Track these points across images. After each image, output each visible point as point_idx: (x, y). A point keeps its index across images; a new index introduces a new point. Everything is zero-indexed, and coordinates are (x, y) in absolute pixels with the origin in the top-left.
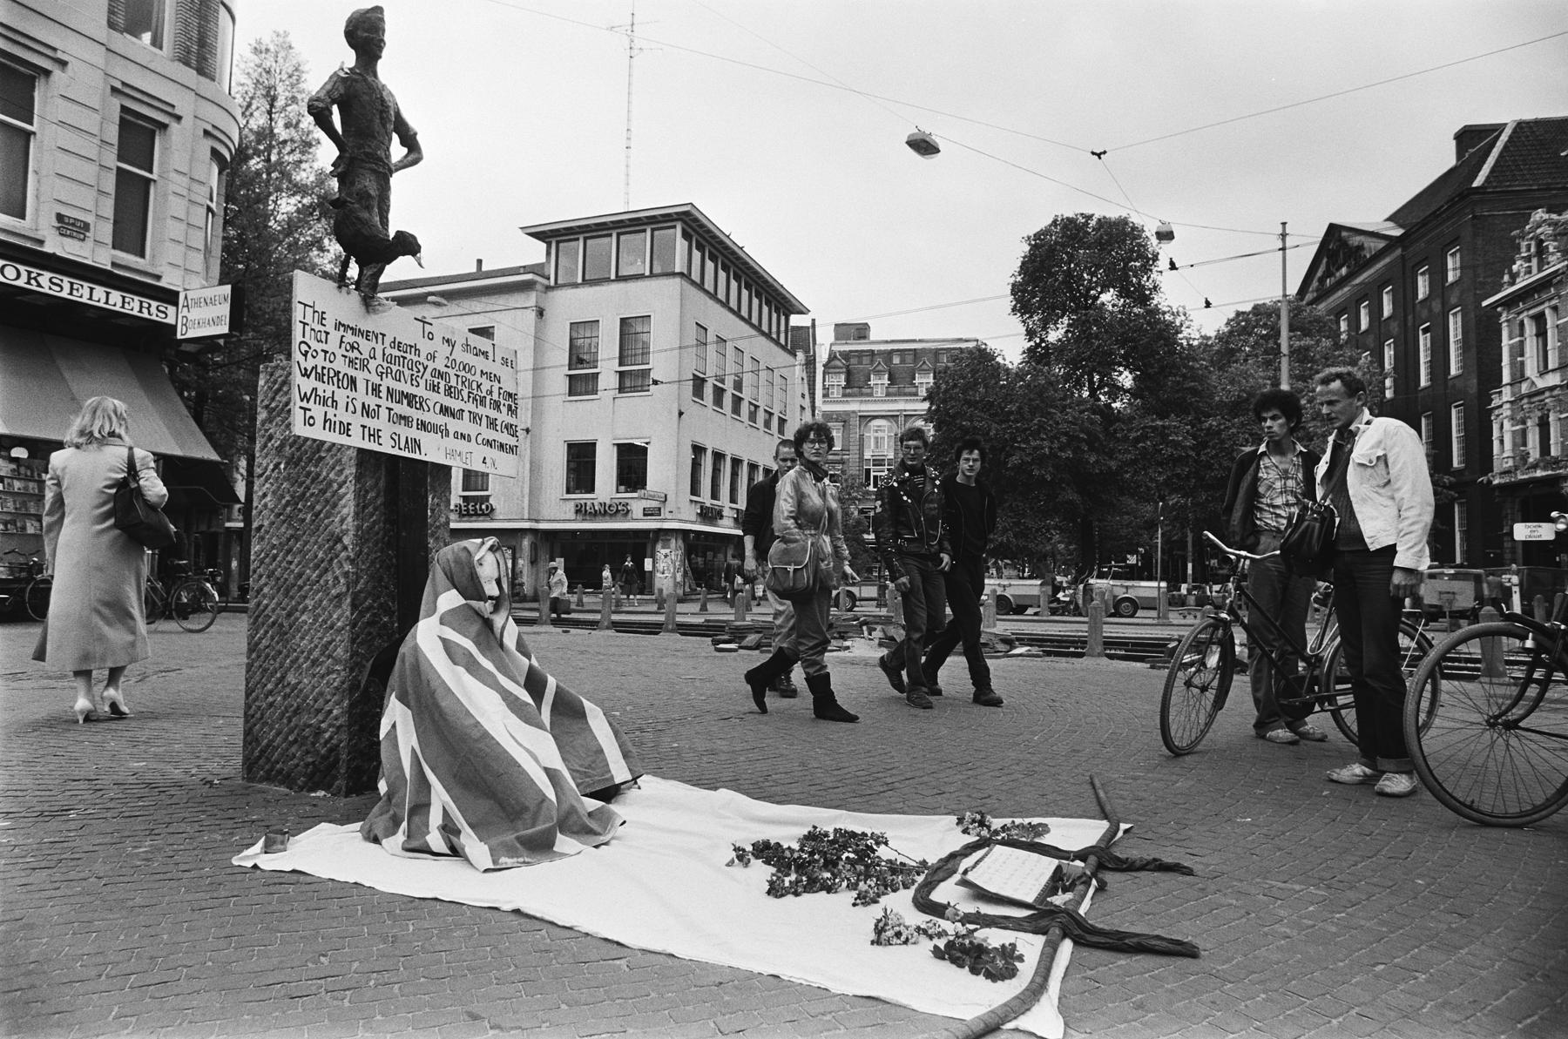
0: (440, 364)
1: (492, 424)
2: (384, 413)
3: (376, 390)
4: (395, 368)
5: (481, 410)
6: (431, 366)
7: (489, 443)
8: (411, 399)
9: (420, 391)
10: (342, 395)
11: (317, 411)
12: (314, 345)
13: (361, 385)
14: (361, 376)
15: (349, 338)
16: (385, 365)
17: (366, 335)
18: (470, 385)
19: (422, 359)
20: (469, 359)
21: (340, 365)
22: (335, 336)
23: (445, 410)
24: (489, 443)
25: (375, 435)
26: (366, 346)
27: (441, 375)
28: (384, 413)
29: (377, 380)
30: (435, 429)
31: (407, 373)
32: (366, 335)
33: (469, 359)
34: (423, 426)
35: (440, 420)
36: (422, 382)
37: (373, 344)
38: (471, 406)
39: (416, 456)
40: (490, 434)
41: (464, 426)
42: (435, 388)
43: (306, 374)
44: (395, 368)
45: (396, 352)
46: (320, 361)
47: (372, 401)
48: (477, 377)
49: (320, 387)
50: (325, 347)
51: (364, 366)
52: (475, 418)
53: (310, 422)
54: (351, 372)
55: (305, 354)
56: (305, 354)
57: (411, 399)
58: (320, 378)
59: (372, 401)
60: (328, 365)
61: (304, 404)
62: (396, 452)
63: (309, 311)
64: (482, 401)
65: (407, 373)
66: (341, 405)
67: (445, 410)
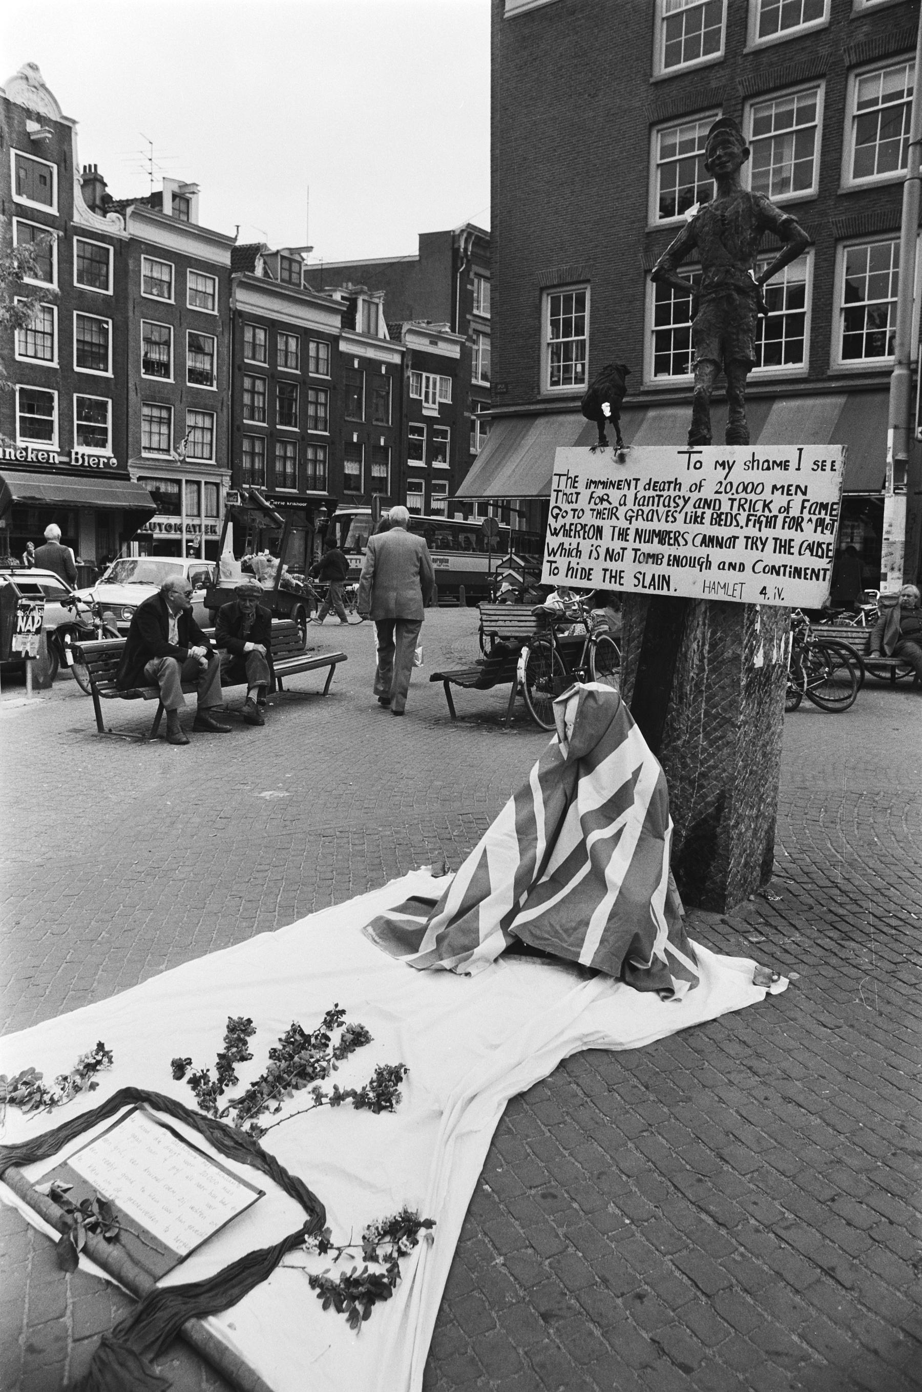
0: (707, 493)
1: (784, 546)
2: (629, 554)
3: (623, 535)
4: (646, 509)
5: (767, 533)
6: (695, 496)
7: (775, 570)
8: (663, 537)
9: (679, 526)
10: (586, 545)
11: (562, 562)
12: (565, 507)
13: (607, 533)
14: (607, 525)
15: (600, 492)
16: (636, 508)
17: (618, 485)
18: (753, 505)
19: (684, 492)
20: (755, 476)
21: (589, 519)
22: (585, 494)
23: (708, 541)
24: (775, 570)
25: (617, 576)
26: (615, 495)
27: (707, 504)
28: (629, 554)
29: (624, 524)
30: (692, 562)
31: (662, 510)
32: (618, 485)
33: (755, 476)
34: (676, 561)
35: (702, 552)
36: (680, 517)
37: (622, 492)
38: (752, 531)
39: (665, 592)
40: (780, 559)
41: (738, 554)
42: (697, 519)
43: (555, 533)
44: (646, 509)
45: (651, 493)
46: (569, 519)
47: (617, 545)
48: (767, 495)
49: (567, 541)
50: (574, 506)
51: (613, 513)
52: (753, 543)
53: (554, 572)
54: (598, 522)
55: (556, 517)
56: (556, 517)
57: (663, 537)
58: (567, 534)
59: (617, 545)
60: (576, 521)
61: (552, 558)
62: (640, 590)
63: (564, 478)
64: (771, 522)
65: (662, 510)
66: (585, 555)
67: (708, 541)
